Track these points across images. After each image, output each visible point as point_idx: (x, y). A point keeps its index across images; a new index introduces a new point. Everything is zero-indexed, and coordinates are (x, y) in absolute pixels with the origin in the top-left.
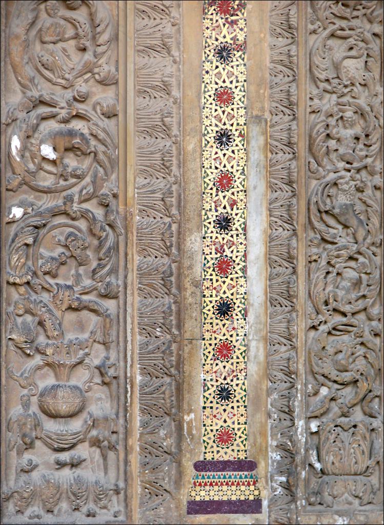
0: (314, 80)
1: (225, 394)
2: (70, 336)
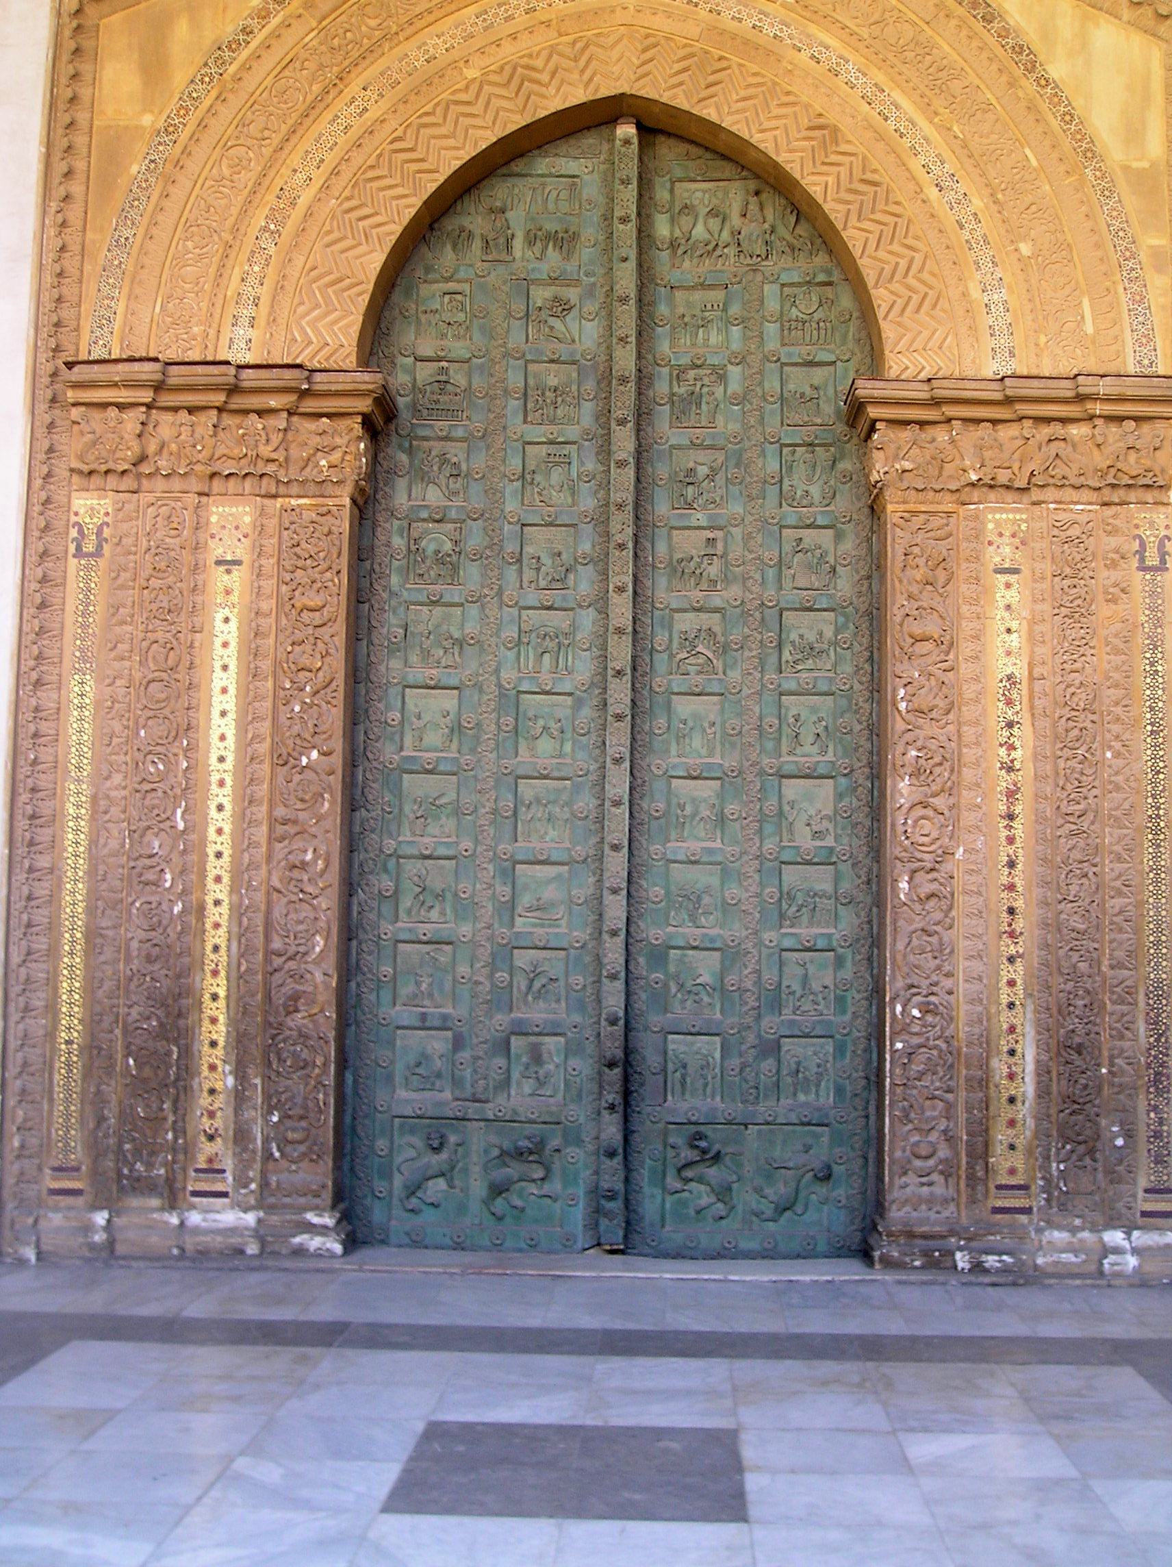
0: (1061, 974)
1: (1012, 1147)
2: (928, 1114)
